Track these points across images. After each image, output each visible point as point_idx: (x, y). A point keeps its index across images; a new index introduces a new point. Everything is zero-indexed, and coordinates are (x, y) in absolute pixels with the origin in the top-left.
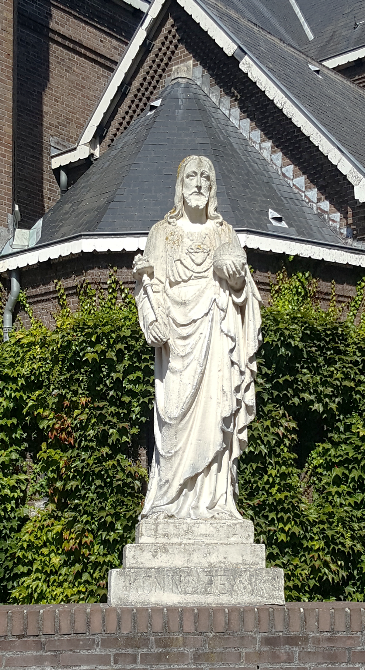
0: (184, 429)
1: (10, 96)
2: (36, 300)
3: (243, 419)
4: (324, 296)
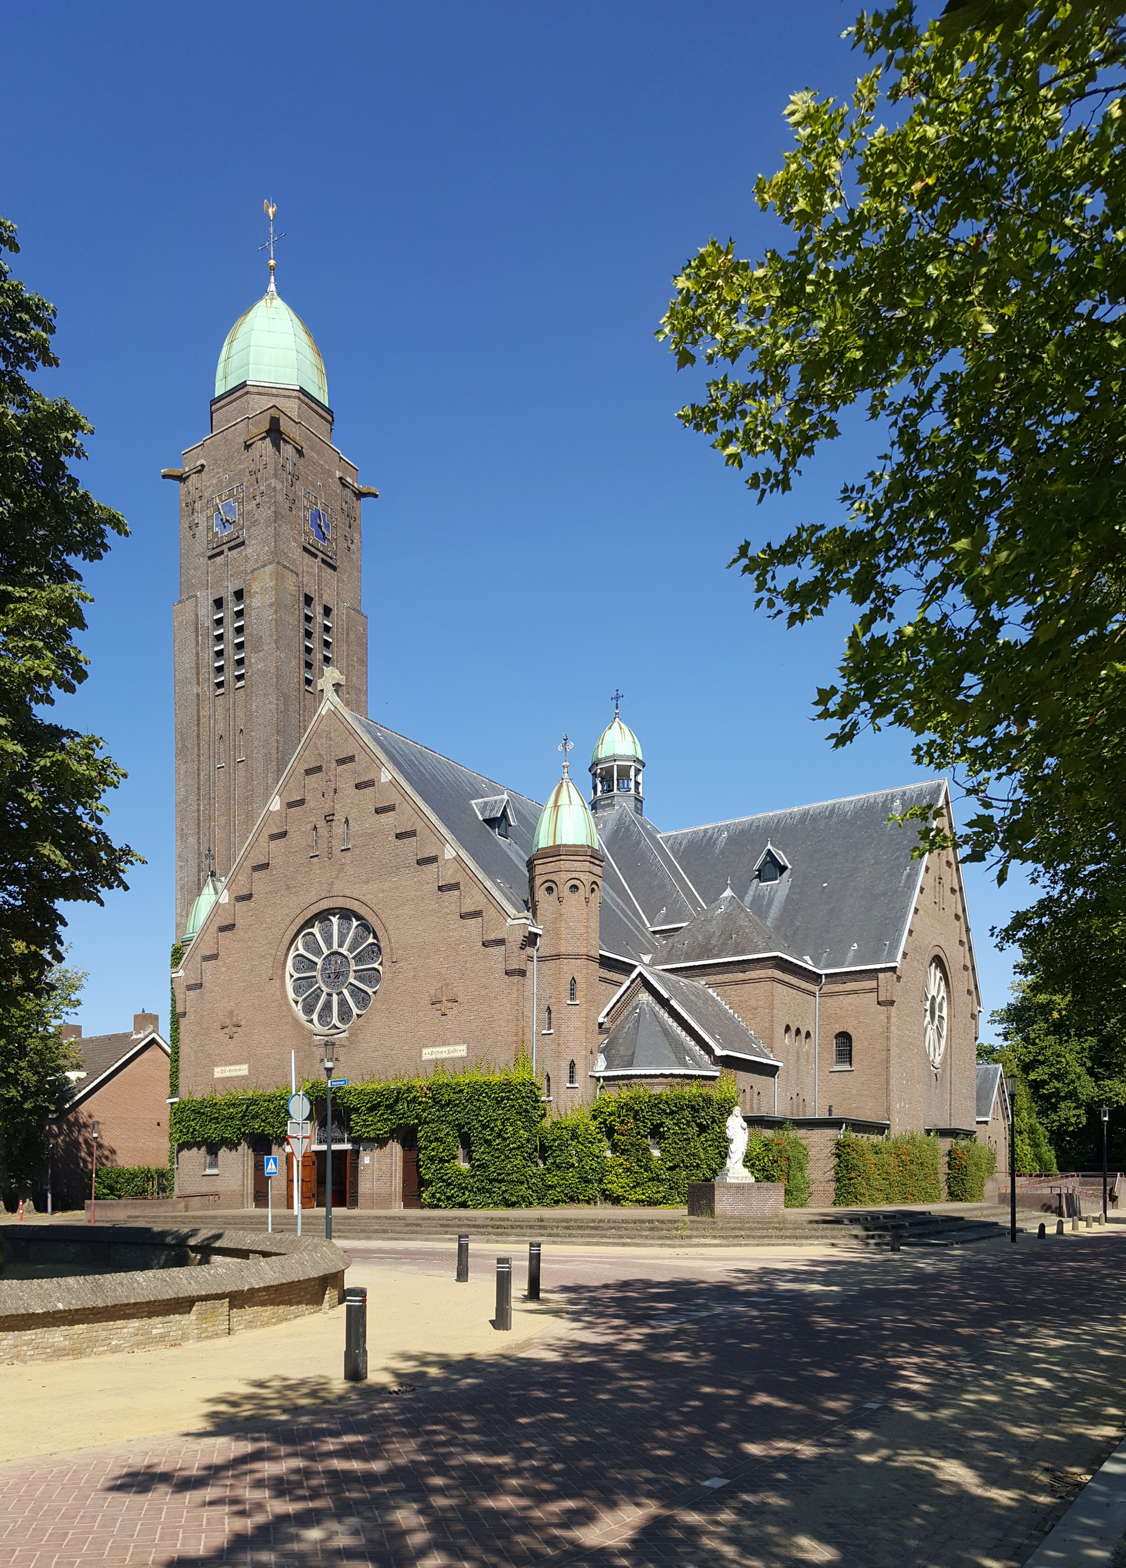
2: (608, 1086)
4: (705, 1085)
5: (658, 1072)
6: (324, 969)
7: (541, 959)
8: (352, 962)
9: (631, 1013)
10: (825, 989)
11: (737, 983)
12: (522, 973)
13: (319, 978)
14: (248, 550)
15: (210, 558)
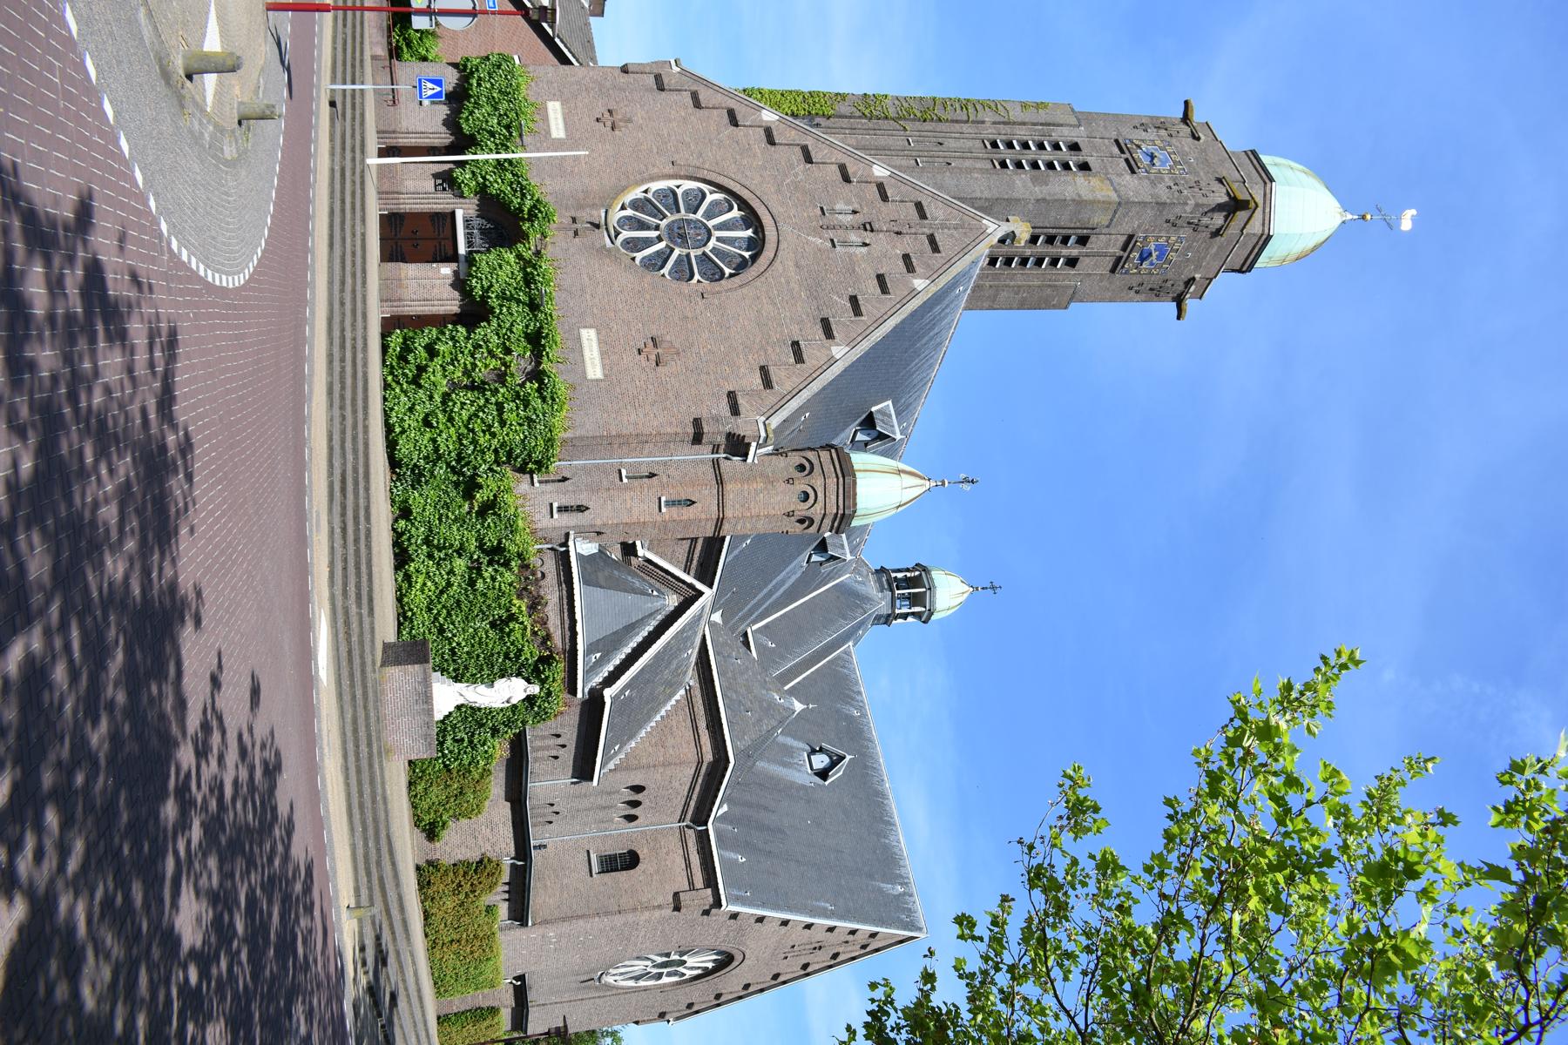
5: (578, 616)
6: (689, 222)
7: (716, 464)
8: (699, 252)
9: (651, 585)
11: (694, 721)
12: (697, 439)
13: (677, 217)
14: (1128, 176)
15: (1117, 141)
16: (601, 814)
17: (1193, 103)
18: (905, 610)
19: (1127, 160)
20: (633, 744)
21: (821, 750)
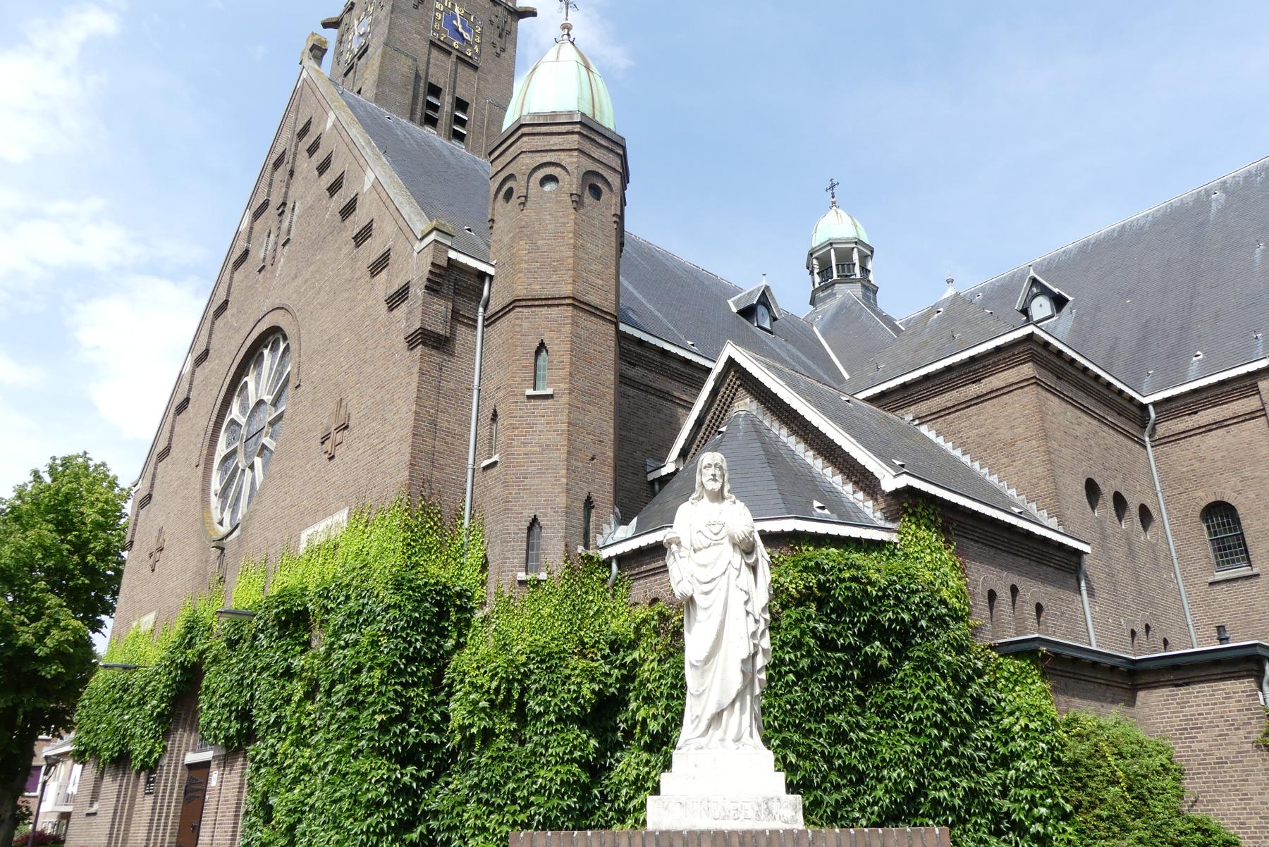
0: (709, 670)
1: (612, 430)
3: (761, 661)
10: (1162, 430)
16: (1143, 558)
17: (325, 18)
18: (857, 269)
19: (359, 58)
20: (1012, 492)
21: (1025, 311)
